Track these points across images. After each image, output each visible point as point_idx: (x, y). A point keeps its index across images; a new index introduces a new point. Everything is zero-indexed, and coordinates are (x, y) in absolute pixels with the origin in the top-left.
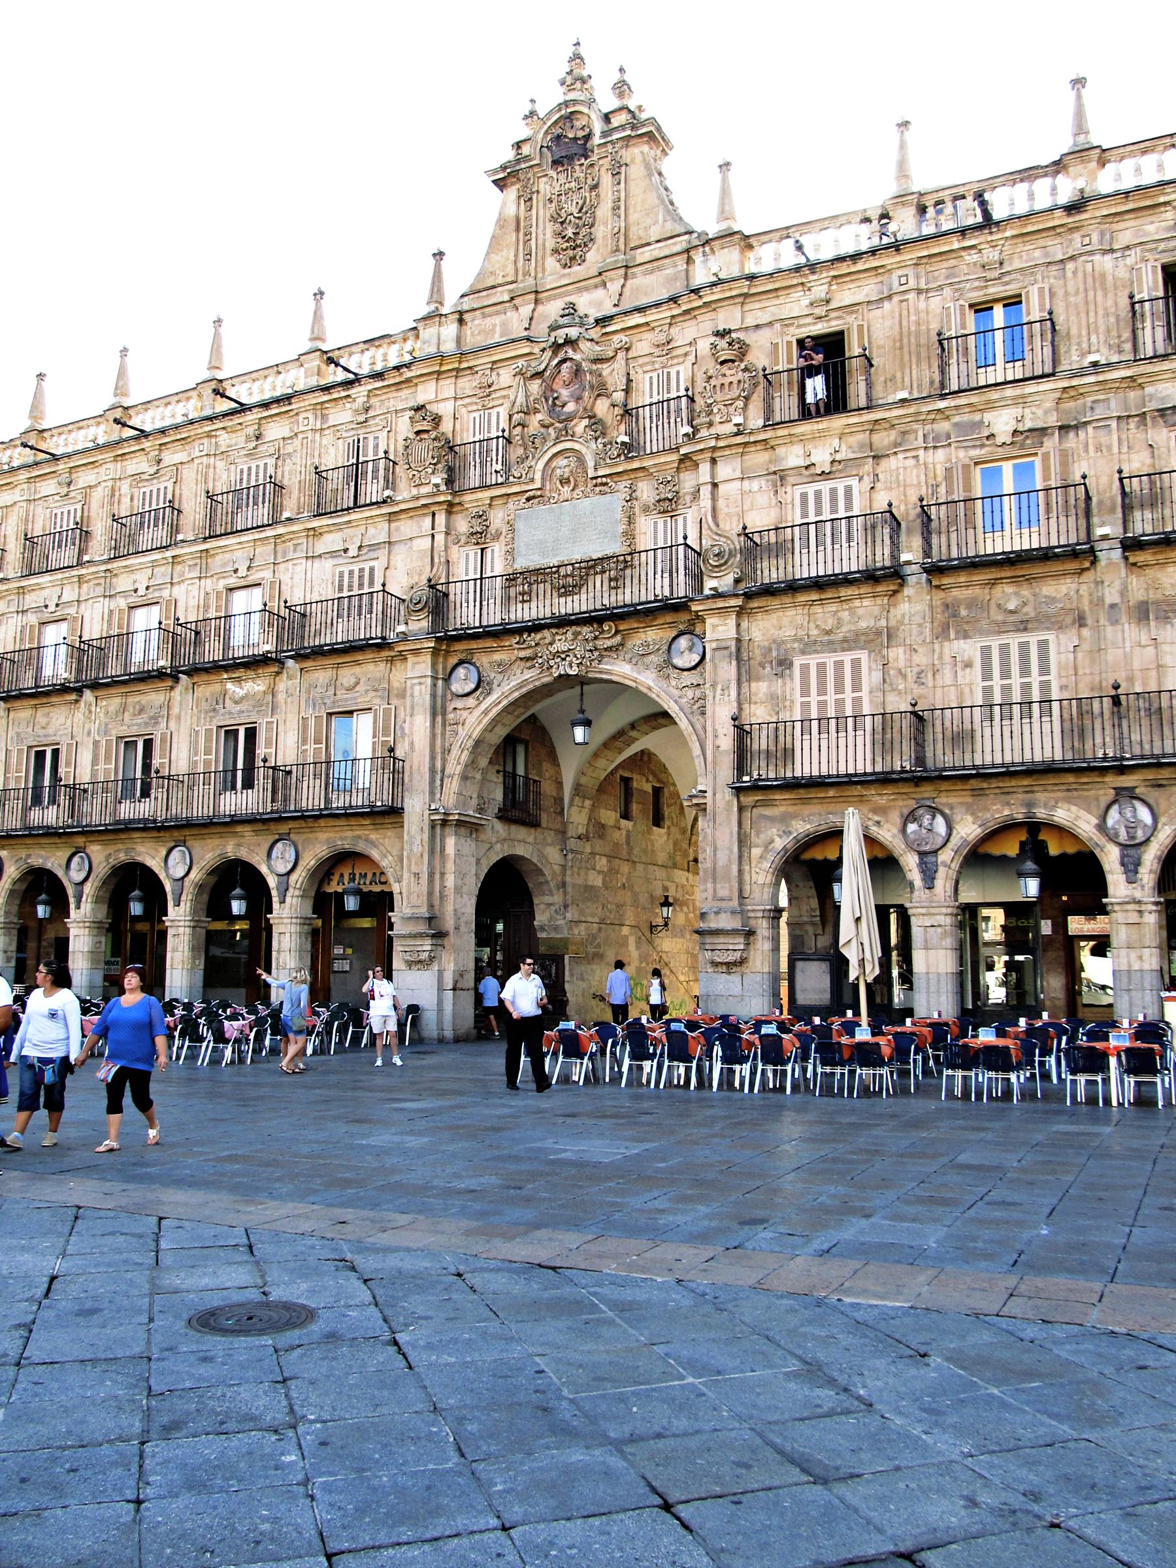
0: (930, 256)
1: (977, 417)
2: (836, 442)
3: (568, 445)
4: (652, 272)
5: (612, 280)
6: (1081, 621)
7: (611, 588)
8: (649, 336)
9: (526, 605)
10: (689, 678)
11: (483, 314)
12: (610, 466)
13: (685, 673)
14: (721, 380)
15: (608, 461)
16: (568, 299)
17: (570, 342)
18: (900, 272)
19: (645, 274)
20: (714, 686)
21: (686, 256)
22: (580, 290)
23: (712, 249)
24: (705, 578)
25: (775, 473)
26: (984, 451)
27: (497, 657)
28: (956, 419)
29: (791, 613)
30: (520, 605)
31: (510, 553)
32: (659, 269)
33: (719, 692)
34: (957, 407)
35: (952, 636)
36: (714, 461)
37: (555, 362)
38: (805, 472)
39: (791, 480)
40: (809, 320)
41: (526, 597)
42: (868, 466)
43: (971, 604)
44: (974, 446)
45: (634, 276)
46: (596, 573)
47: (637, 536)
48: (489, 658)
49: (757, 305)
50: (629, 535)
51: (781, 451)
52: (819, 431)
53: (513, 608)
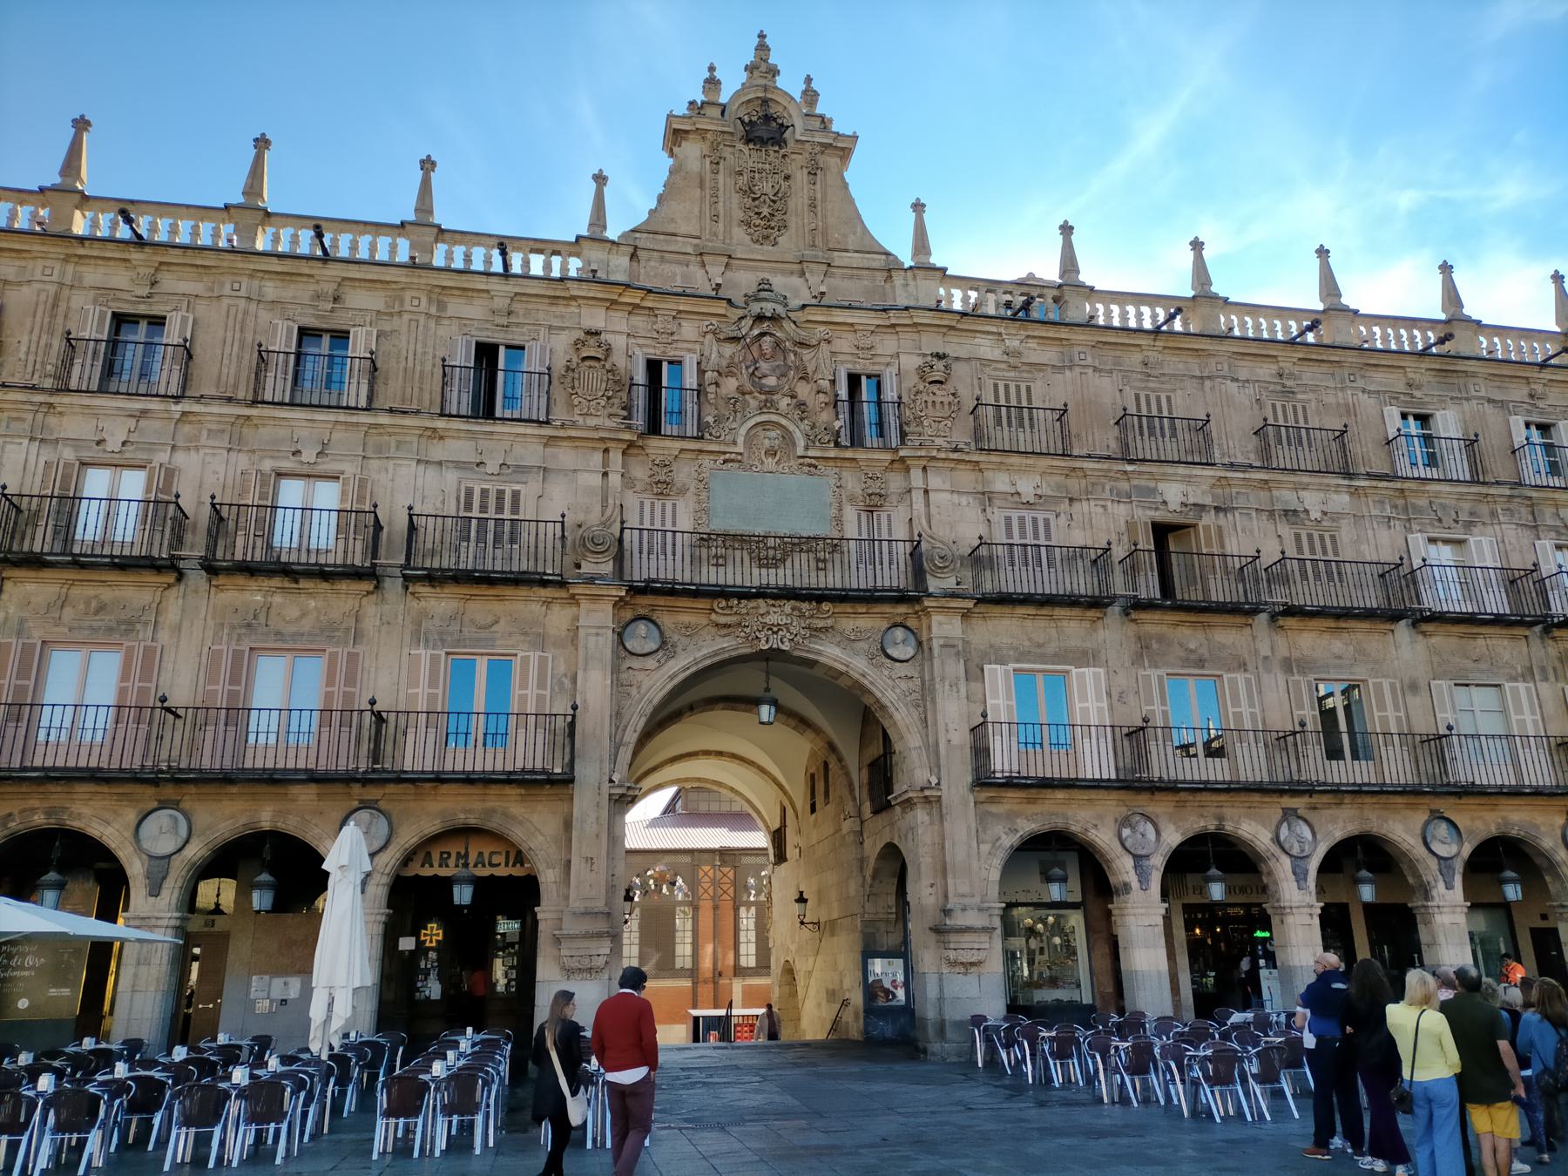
0: (1105, 343)
1: (1152, 484)
2: (1038, 478)
3: (774, 418)
4: (851, 277)
5: (811, 272)
6: (1243, 666)
7: (818, 569)
8: (850, 336)
9: (721, 570)
10: (902, 670)
11: (662, 257)
13: (898, 664)
14: (930, 399)
16: (767, 275)
17: (775, 319)
18: (1080, 349)
19: (843, 277)
20: (943, 679)
21: (885, 274)
22: (774, 271)
23: (915, 276)
24: (928, 577)
25: (983, 493)
26: (1157, 514)
27: (686, 618)
28: (1135, 482)
29: (1006, 622)
30: (713, 569)
31: (703, 510)
32: (859, 278)
33: (947, 687)
34: (1141, 473)
35: (1146, 664)
36: (924, 468)
37: (756, 332)
38: (1009, 497)
39: (997, 502)
40: (1003, 366)
41: (719, 562)
42: (1064, 506)
43: (1161, 639)
44: (1151, 508)
45: (833, 275)
46: (801, 551)
48: (677, 618)
49: (956, 340)
50: (839, 521)
51: (989, 474)
52: (1027, 465)
53: (704, 570)
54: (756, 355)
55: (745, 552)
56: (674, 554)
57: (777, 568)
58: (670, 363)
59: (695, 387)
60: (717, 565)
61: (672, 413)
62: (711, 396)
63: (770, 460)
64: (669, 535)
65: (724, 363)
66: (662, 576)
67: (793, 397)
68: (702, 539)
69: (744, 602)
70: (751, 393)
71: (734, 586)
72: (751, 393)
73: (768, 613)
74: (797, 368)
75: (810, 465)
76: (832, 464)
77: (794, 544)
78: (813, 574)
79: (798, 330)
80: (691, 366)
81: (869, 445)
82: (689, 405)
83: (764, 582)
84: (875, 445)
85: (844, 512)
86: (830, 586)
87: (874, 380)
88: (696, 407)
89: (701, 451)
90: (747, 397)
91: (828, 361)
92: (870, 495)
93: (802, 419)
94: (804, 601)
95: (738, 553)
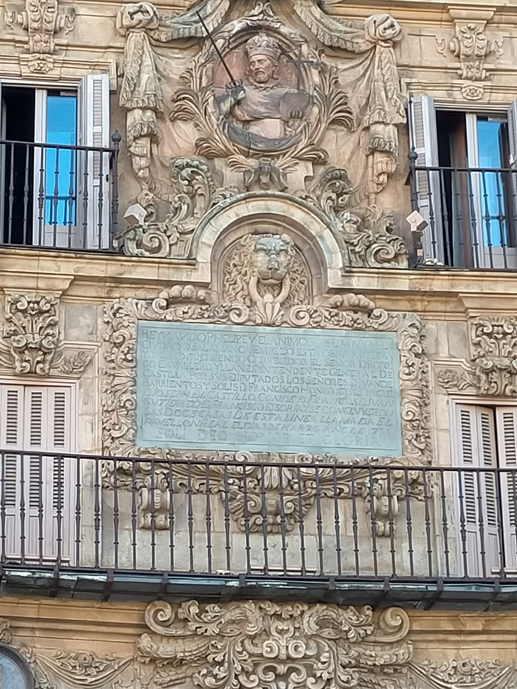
7: (376, 535)
12: (381, 274)
15: (372, 262)
46: (337, 496)
47: (434, 434)
54: (236, 74)
55: (215, 500)
56: (59, 506)
57: (284, 532)
58: (53, 92)
59: (105, 143)
60: (153, 528)
61: (55, 198)
62: (140, 162)
63: (268, 297)
64: (48, 463)
65: (169, 91)
66: (32, 554)
67: (317, 162)
68: (121, 471)
69: (213, 609)
70: (226, 155)
71: (191, 575)
72: (226, 155)
73: (266, 633)
74: (326, 100)
75: (356, 308)
76: (404, 304)
77: (322, 481)
78: (365, 546)
79: (326, 20)
80: (98, 100)
81: (484, 262)
82: (92, 182)
83: (257, 564)
84: (498, 264)
85: (431, 408)
86: (403, 572)
87: (494, 126)
88: (106, 186)
89: (118, 281)
90: (218, 163)
91: (393, 85)
92: (488, 372)
93: (337, 210)
94: (344, 606)
95: (198, 501)
